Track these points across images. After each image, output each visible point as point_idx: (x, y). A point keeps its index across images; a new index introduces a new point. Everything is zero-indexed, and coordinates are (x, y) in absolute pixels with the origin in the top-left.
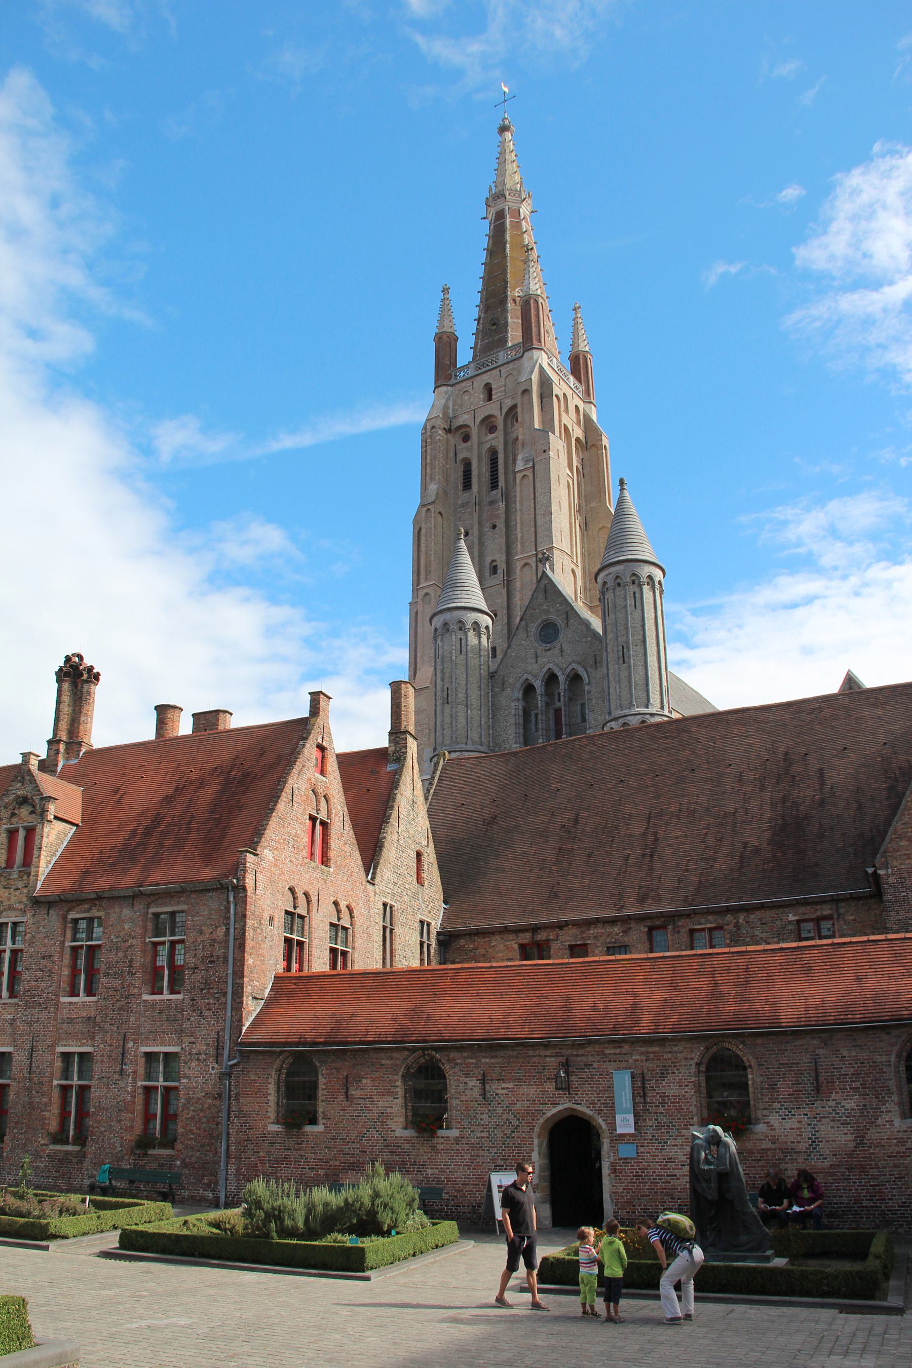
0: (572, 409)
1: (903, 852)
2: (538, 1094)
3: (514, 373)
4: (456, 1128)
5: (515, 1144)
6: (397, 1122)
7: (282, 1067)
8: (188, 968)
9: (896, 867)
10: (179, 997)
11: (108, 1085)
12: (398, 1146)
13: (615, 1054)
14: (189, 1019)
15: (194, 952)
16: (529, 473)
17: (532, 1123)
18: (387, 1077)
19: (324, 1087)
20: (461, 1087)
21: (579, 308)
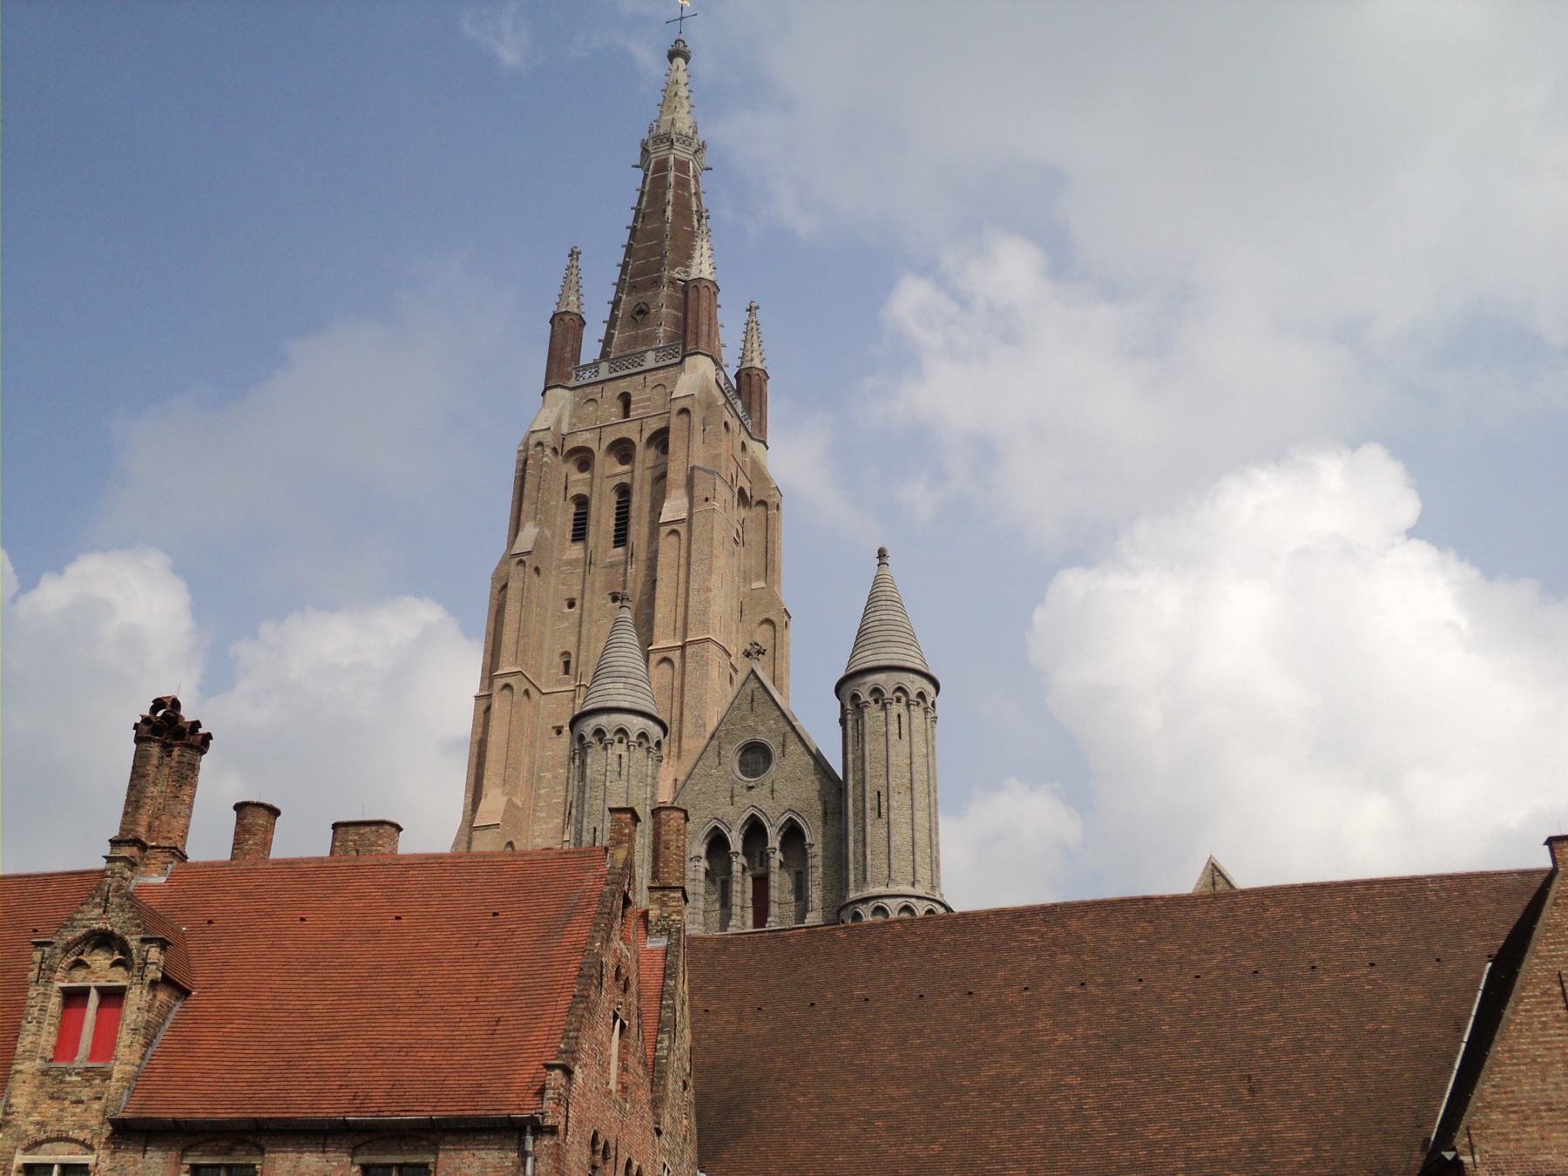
1: (1496, 1130)
9: (1487, 1152)
16: (682, 529)
21: (757, 308)
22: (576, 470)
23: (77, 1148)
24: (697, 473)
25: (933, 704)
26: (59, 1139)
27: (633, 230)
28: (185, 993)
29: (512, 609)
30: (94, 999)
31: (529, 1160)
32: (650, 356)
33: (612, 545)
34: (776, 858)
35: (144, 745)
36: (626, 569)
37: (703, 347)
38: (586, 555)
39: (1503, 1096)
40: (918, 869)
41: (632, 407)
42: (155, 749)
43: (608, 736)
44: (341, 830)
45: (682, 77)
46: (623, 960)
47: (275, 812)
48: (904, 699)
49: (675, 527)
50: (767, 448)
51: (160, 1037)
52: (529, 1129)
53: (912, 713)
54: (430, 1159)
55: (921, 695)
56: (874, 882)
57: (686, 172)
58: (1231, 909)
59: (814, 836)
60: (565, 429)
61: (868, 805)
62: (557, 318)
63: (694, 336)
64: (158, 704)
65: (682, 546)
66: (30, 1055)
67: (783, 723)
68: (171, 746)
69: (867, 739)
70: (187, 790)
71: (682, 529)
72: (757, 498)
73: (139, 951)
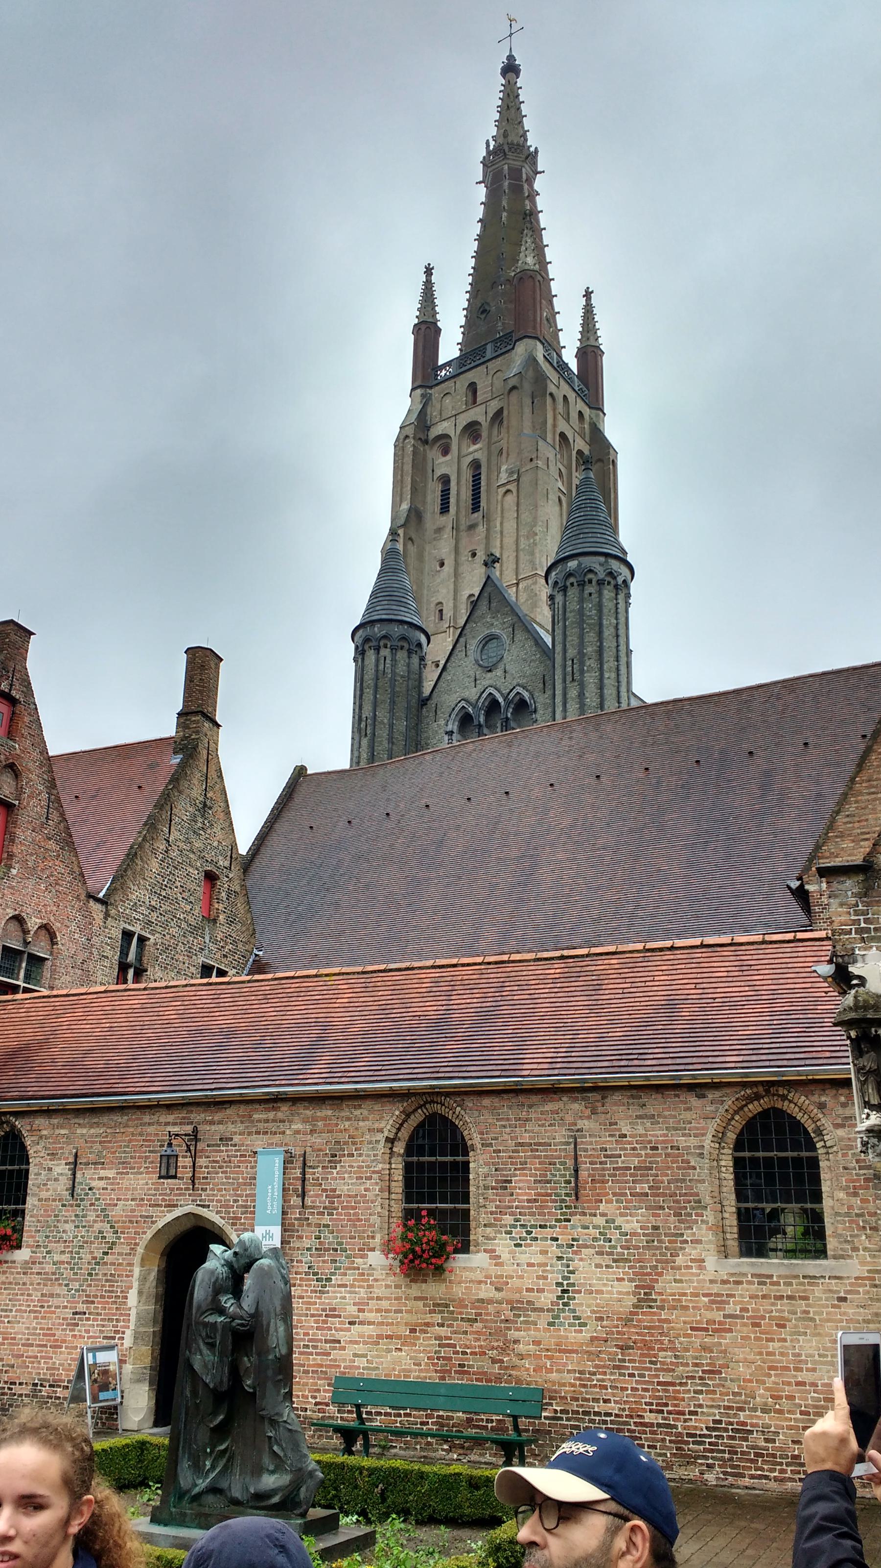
0: (574, 415)
2: (149, 1189)
5: (106, 1274)
13: (267, 1121)
16: (512, 487)
17: (135, 1239)
20: (42, 1177)
22: (440, 456)
33: (471, 511)
39: (857, 825)
57: (520, 178)
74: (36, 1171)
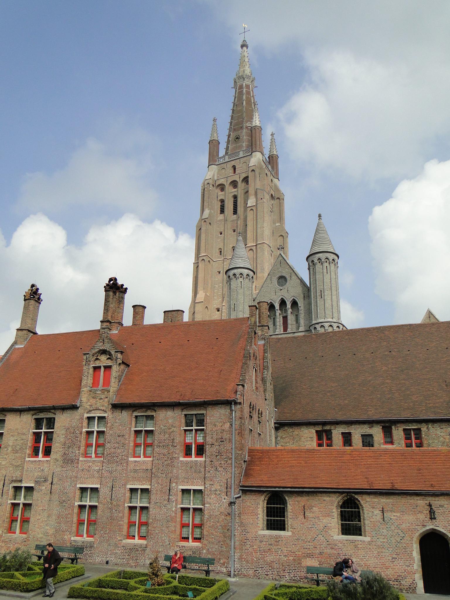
2: (414, 520)
3: (247, 162)
4: (369, 536)
5: (402, 546)
6: (334, 532)
7: (265, 499)
8: (208, 444)
10: (203, 459)
11: (160, 507)
12: (335, 545)
14: (209, 472)
15: (211, 436)
17: (412, 535)
18: (327, 507)
19: (291, 511)
20: (370, 514)
21: (274, 134)
22: (220, 191)
23: (102, 412)
24: (258, 191)
25: (337, 263)
26: (96, 409)
27: (233, 110)
28: (128, 366)
29: (203, 236)
30: (102, 369)
31: (234, 412)
32: (241, 153)
34: (290, 311)
35: (108, 293)
36: (237, 222)
37: (258, 148)
38: (225, 218)
40: (334, 313)
41: (236, 170)
42: (111, 293)
43: (237, 276)
44: (167, 313)
45: (246, 54)
46: (255, 351)
47: (144, 307)
48: (328, 261)
49: (252, 208)
50: (279, 181)
51: (122, 379)
52: (233, 403)
53: (331, 266)
54: (204, 412)
55: (333, 260)
56: (320, 318)
57: (249, 89)
58: (438, 328)
59: (301, 304)
60: (216, 179)
61: (318, 295)
62: (211, 142)
63: (255, 145)
64: (111, 280)
65: (254, 214)
66: (86, 386)
67: (290, 270)
68: (116, 292)
69: (317, 274)
70: (121, 305)
71: (254, 208)
72: (276, 197)
73: (115, 355)
74: (367, 512)
